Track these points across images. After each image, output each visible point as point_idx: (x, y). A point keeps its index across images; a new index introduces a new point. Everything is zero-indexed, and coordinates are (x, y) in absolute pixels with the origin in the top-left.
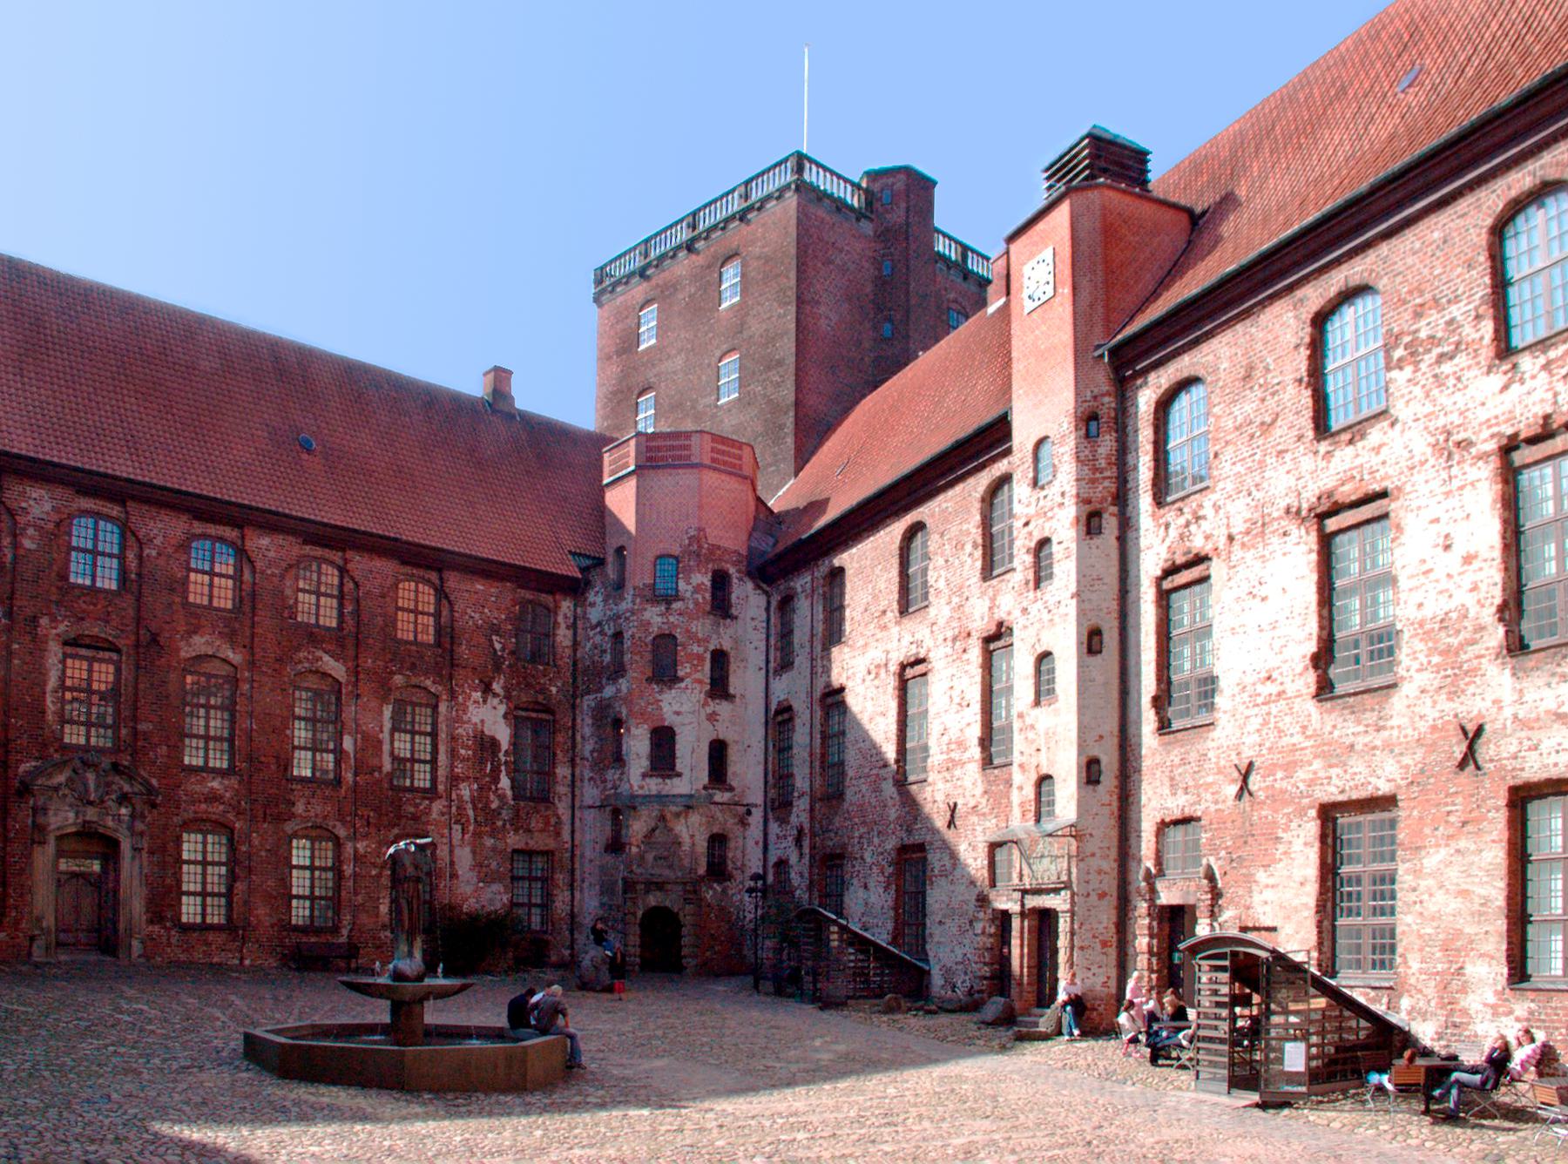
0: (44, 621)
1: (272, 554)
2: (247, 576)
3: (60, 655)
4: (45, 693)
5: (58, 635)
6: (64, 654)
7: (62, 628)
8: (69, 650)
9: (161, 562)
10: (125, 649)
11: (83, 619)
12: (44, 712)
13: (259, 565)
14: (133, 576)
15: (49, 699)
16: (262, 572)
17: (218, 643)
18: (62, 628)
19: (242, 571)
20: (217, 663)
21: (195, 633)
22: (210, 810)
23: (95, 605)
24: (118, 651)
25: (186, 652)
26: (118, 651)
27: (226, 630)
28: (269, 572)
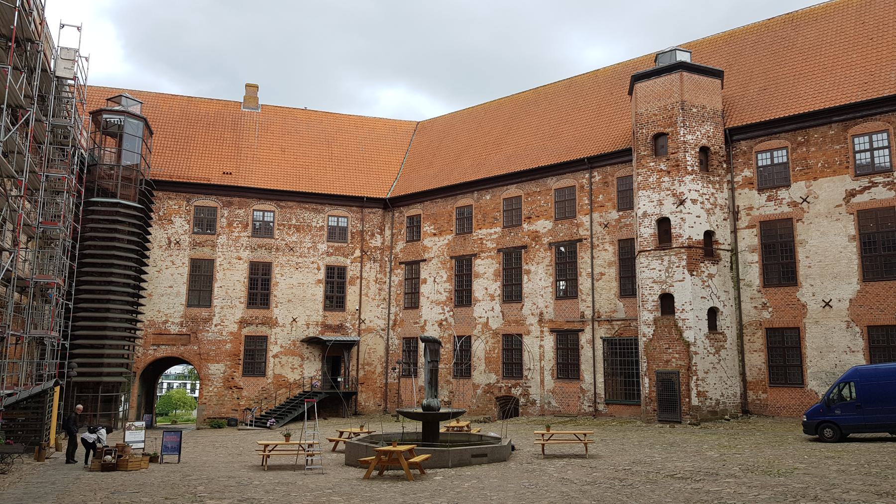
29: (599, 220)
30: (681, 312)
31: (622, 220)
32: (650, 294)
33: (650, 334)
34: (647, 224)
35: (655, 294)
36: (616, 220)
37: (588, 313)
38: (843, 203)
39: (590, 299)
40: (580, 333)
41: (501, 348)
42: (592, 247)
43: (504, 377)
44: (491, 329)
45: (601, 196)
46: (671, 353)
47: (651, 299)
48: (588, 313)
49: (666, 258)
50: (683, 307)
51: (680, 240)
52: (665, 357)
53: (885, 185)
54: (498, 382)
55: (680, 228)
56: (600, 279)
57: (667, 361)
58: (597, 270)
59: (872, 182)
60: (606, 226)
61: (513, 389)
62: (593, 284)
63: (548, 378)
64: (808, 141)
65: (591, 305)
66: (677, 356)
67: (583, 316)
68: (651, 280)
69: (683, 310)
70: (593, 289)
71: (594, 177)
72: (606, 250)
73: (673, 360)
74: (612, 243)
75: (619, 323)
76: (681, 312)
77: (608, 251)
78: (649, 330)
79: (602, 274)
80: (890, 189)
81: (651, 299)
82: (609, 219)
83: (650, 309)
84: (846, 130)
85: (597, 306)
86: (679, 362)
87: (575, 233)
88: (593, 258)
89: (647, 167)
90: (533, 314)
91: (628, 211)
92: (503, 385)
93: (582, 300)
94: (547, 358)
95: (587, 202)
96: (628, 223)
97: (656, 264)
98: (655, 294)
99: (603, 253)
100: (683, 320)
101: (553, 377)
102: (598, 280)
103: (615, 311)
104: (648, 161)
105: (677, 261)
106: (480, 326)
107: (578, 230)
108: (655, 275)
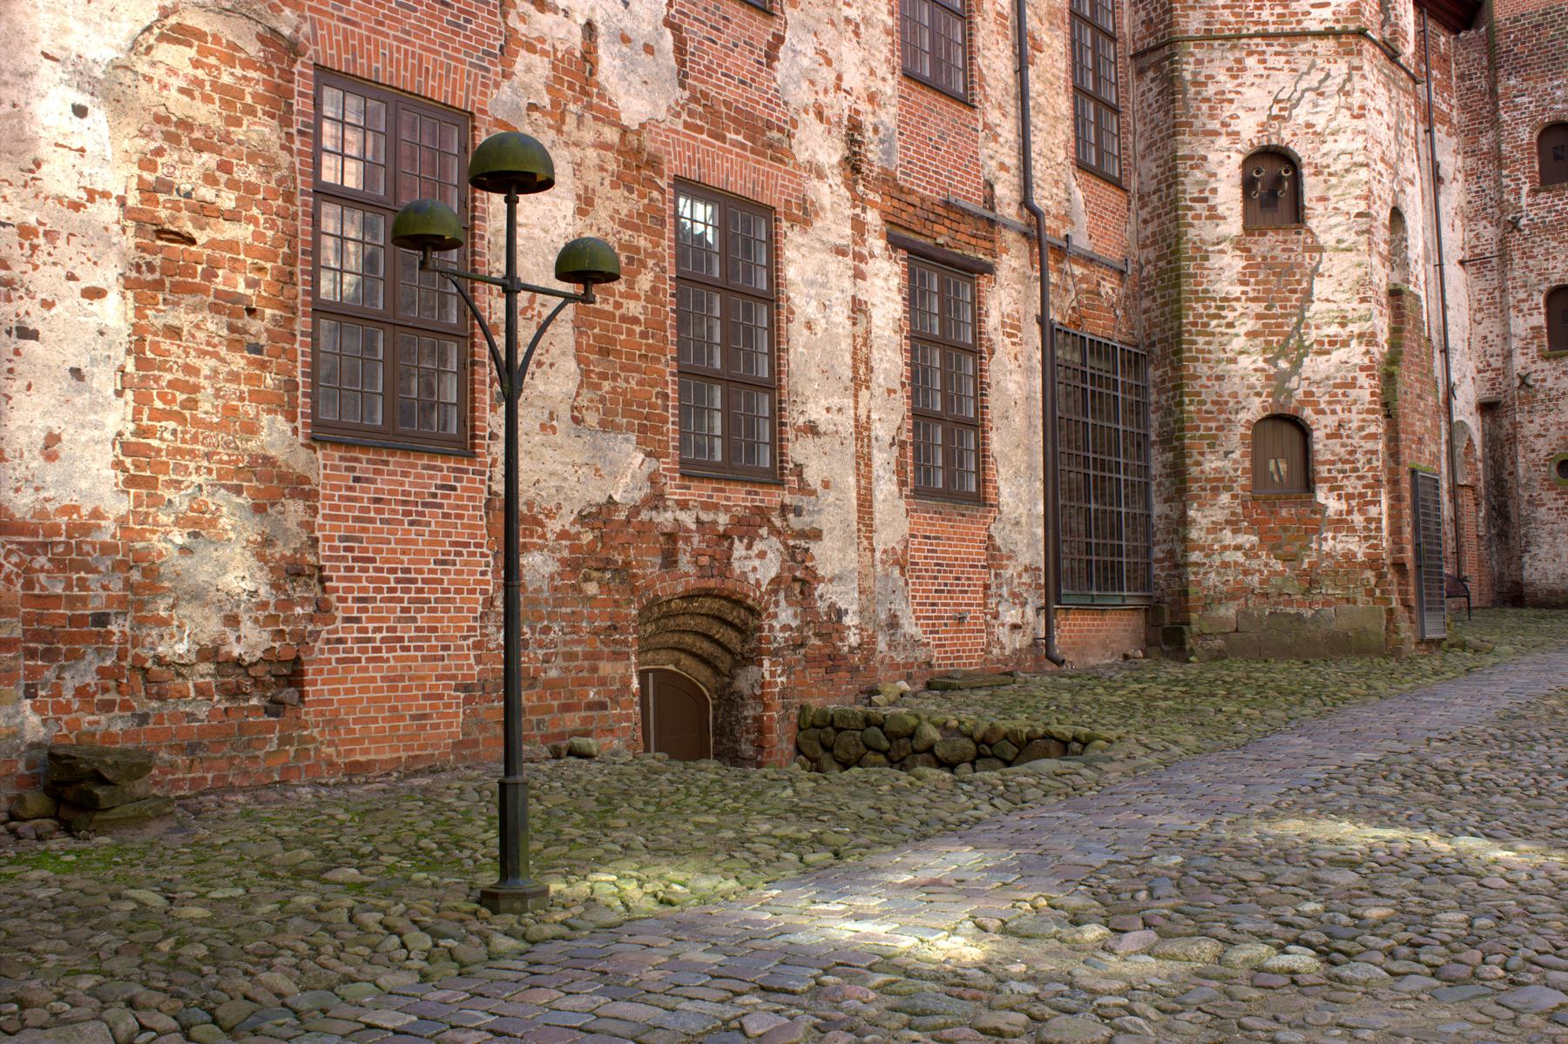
41: (669, 264)
43: (691, 471)
44: (609, 117)
54: (656, 500)
61: (739, 549)
63: (886, 489)
90: (820, 115)
92: (688, 519)
94: (879, 378)
101: (902, 483)
106: (543, 67)
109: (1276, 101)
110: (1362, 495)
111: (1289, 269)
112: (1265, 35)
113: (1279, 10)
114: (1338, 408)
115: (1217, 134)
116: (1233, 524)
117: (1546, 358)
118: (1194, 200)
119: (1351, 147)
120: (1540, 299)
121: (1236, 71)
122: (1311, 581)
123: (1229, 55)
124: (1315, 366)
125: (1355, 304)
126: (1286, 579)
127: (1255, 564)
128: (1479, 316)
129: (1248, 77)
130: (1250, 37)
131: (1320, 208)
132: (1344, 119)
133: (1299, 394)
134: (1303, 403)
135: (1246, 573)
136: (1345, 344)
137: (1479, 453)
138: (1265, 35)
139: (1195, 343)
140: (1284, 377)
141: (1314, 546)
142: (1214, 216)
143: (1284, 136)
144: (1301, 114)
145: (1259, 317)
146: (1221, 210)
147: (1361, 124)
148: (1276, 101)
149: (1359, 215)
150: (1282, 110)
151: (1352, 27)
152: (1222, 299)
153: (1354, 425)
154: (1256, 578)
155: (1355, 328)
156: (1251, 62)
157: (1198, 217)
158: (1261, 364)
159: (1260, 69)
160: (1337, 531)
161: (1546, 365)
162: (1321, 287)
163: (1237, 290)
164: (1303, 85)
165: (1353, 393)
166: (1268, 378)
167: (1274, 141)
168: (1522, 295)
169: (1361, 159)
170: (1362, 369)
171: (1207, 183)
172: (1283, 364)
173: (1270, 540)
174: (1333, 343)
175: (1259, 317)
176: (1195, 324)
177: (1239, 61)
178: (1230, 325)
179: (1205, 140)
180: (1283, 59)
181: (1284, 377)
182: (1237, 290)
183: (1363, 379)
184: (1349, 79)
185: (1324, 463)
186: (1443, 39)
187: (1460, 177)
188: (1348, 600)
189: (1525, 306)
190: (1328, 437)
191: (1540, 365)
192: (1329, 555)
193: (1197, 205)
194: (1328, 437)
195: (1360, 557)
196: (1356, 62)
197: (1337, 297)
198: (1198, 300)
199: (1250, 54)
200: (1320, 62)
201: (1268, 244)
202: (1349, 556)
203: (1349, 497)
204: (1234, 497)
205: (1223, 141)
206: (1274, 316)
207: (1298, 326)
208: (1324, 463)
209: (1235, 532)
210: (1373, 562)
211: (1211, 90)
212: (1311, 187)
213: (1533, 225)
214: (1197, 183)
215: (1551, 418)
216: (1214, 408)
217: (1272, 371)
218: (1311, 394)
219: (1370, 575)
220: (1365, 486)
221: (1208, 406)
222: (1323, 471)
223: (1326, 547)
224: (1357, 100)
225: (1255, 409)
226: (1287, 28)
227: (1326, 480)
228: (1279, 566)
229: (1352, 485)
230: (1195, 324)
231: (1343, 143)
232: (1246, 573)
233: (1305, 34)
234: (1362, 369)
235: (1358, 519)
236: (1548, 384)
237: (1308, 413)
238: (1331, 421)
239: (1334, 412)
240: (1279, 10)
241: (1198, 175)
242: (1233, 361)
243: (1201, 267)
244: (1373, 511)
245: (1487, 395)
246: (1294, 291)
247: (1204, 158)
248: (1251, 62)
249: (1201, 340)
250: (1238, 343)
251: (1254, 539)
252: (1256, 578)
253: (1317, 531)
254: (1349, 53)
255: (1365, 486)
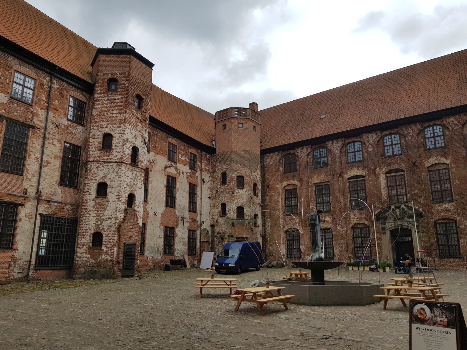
0: (378, 169)
1: (455, 122)
2: (447, 133)
3: (385, 177)
4: (381, 189)
5: (383, 172)
6: (386, 176)
7: (384, 170)
8: (388, 175)
9: (413, 140)
10: (405, 170)
11: (390, 165)
12: (381, 195)
13: (450, 128)
14: (405, 147)
15: (382, 190)
16: (452, 129)
17: (439, 158)
18: (384, 170)
19: (445, 132)
20: (441, 165)
21: (430, 158)
22: (445, 215)
23: (394, 160)
24: (403, 171)
25: (427, 164)
26: (403, 171)
27: (442, 153)
28: (455, 129)
29: (53, 119)
30: (138, 207)
31: (70, 128)
32: (124, 192)
33: (121, 218)
34: (128, 147)
35: (127, 193)
36: (65, 126)
37: (32, 192)
38: (164, 169)
39: (35, 179)
40: (20, 208)
42: (44, 138)
45: (56, 101)
46: (133, 232)
47: (124, 195)
48: (32, 192)
49: (135, 172)
50: (139, 204)
51: (142, 164)
52: (130, 234)
53: (175, 168)
55: (143, 157)
56: (46, 166)
57: (131, 237)
58: (45, 158)
59: (171, 164)
60: (57, 126)
62: (40, 168)
64: (157, 134)
65: (35, 184)
66: (135, 234)
67: (25, 192)
68: (126, 183)
69: (139, 206)
70: (40, 173)
71: (54, 83)
72: (54, 145)
73: (134, 236)
74: (59, 141)
75: (56, 204)
76: (138, 207)
77: (56, 147)
78: (121, 215)
79: (48, 163)
80: (175, 170)
81: (124, 195)
82: (59, 122)
83: (123, 201)
84: (167, 138)
85: (41, 187)
86: (136, 238)
87: (29, 119)
88: (43, 147)
89: (131, 111)
91: (74, 124)
93: (27, 178)
95: (44, 99)
96: (73, 132)
97: (129, 173)
98: (127, 193)
99: (52, 146)
100: (139, 212)
102: (44, 166)
103: (54, 194)
104: (133, 108)
105: (139, 176)
107: (32, 117)
108: (128, 180)
109: (104, 174)
110: (111, 248)
111: (103, 205)
112: (104, 162)
113: (107, 157)
114: (108, 231)
115: (93, 179)
116: (86, 253)
117: (221, 217)
118: (86, 191)
119: (117, 183)
120: (220, 205)
121: (98, 168)
122: (99, 263)
123: (97, 165)
124: (105, 223)
125: (114, 212)
126: (94, 264)
127: (89, 260)
128: (212, 208)
129: (100, 169)
130: (101, 162)
131: (110, 194)
132: (117, 178)
133: (101, 228)
134: (102, 230)
135: (87, 262)
136: (111, 219)
137: (210, 234)
138: (104, 162)
139: (83, 218)
140: (99, 225)
141: (101, 257)
142: (90, 194)
143: (105, 180)
144: (109, 176)
145: (96, 213)
146: (91, 193)
147: (119, 179)
148: (104, 174)
149: (117, 195)
150: (105, 175)
151: (120, 161)
152: (89, 210)
153: (111, 234)
154: (89, 263)
155: (113, 216)
156: (101, 166)
157: (87, 194)
158: (95, 222)
159: (102, 168)
160: (105, 254)
161: (220, 218)
162: (108, 208)
163: (92, 208)
164: (110, 171)
165: (111, 228)
166: (96, 225)
167: (103, 181)
168: (217, 205)
169: (119, 185)
170: (114, 224)
171: (89, 188)
172: (99, 223)
173: (93, 256)
174: (109, 219)
175: (96, 213)
176: (83, 214)
177: (98, 166)
178: (90, 215)
179: (90, 180)
180: (107, 166)
181: (99, 225)
182: (92, 208)
183: (114, 225)
184: (119, 170)
185: (104, 241)
186: (208, 155)
187: (210, 181)
188: (105, 268)
189: (218, 207)
190: (106, 236)
191: (220, 218)
192: (103, 259)
193: (87, 192)
194: (106, 236)
195: (109, 260)
196: (120, 167)
197: (111, 210)
198: (84, 210)
199: (101, 165)
200: (113, 167)
201: (99, 200)
202: (107, 259)
203: (108, 248)
204: (86, 247)
205: (94, 181)
206: (99, 213)
207: (103, 215)
208: (104, 241)
209: (86, 254)
210: (112, 261)
211: (92, 171)
212: (109, 190)
213: (220, 192)
214: (88, 188)
215: (221, 228)
216: (85, 230)
217: (97, 224)
218: (104, 228)
219: (111, 263)
220: (112, 246)
221: (84, 230)
222: (104, 243)
223: (103, 257)
224: (119, 174)
225: (93, 231)
226: (108, 161)
227: (104, 245)
228: (93, 261)
229: (109, 246)
230: (83, 214)
231: (116, 182)
232: (87, 262)
233: (111, 162)
234: (114, 224)
235: (109, 252)
236: (220, 222)
237: (102, 232)
238: (106, 233)
239: (107, 232)
240: (107, 157)
241: (88, 187)
242: (90, 221)
243: (86, 204)
244: (112, 251)
245: (212, 223)
246: (103, 209)
247: (89, 184)
248: (101, 166)
249: (84, 217)
250: (91, 218)
251: (89, 256)
252: (89, 263)
253: (101, 254)
254: (119, 166)
255: (112, 246)
